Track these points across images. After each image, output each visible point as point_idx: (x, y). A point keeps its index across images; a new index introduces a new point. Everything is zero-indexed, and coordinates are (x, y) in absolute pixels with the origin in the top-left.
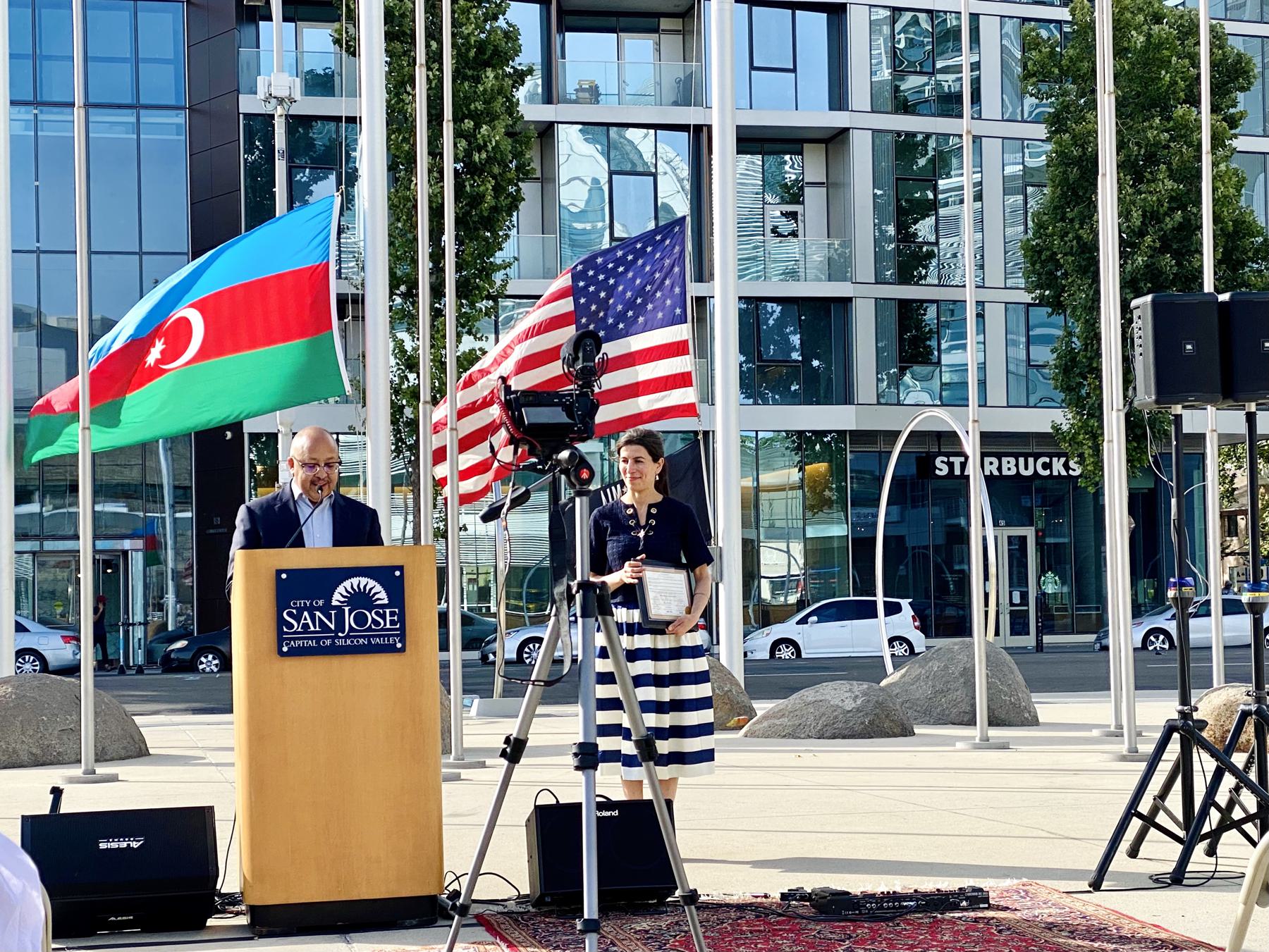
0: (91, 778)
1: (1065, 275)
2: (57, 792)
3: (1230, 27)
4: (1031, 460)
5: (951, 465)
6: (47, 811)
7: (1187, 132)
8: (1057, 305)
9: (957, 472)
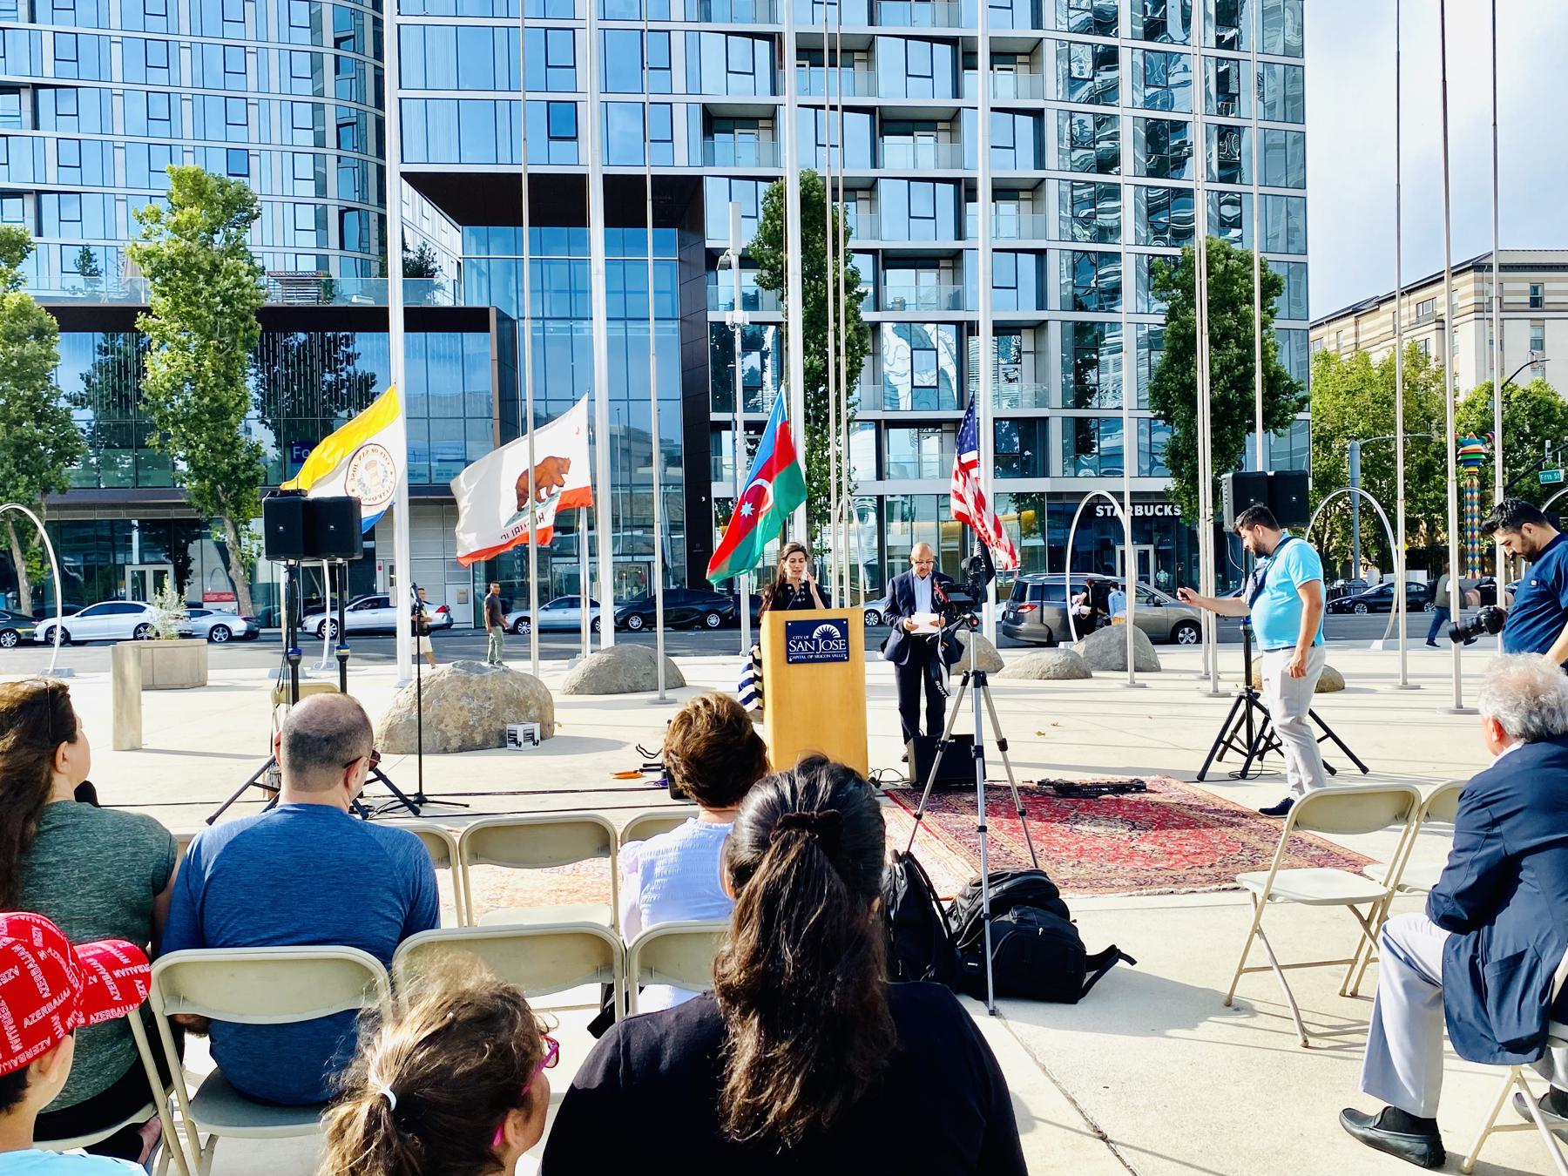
1: (1173, 403)
3: (1269, 257)
4: (1152, 507)
5: (1105, 511)
7: (1246, 321)
8: (1168, 419)
9: (1109, 514)
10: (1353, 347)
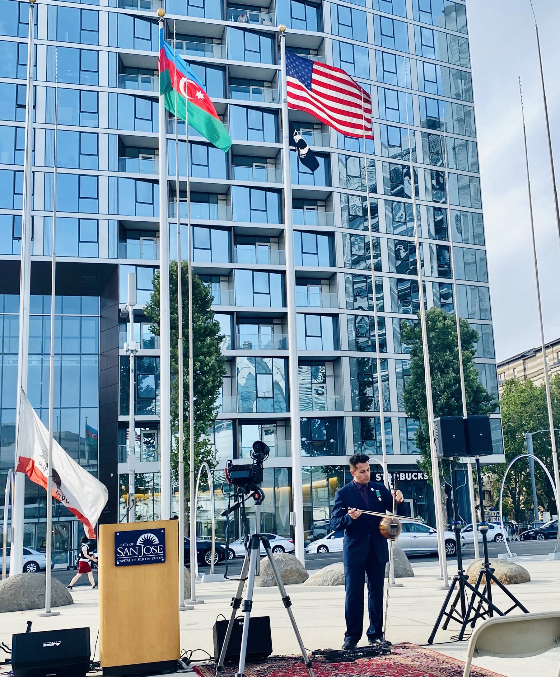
0: (49, 614)
2: (29, 623)
6: (25, 632)
10: (523, 378)
